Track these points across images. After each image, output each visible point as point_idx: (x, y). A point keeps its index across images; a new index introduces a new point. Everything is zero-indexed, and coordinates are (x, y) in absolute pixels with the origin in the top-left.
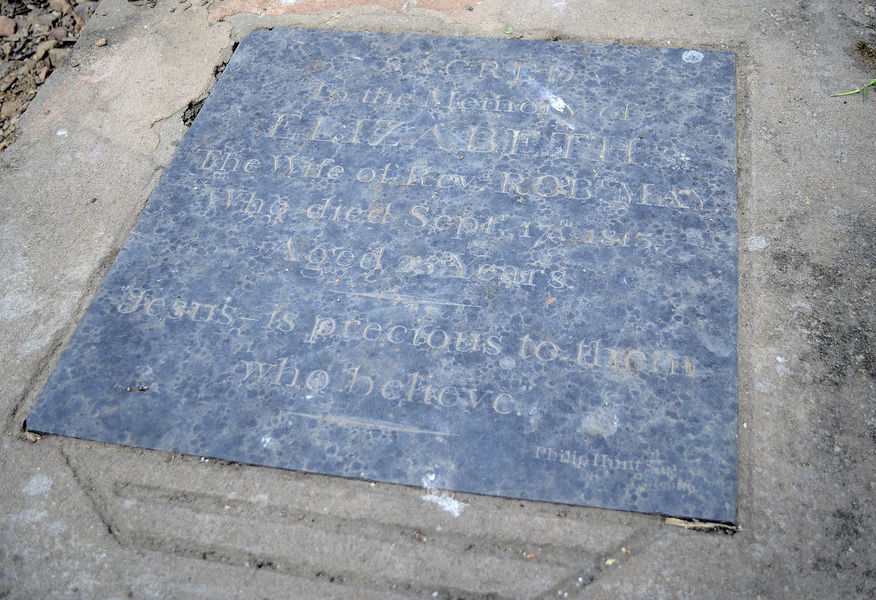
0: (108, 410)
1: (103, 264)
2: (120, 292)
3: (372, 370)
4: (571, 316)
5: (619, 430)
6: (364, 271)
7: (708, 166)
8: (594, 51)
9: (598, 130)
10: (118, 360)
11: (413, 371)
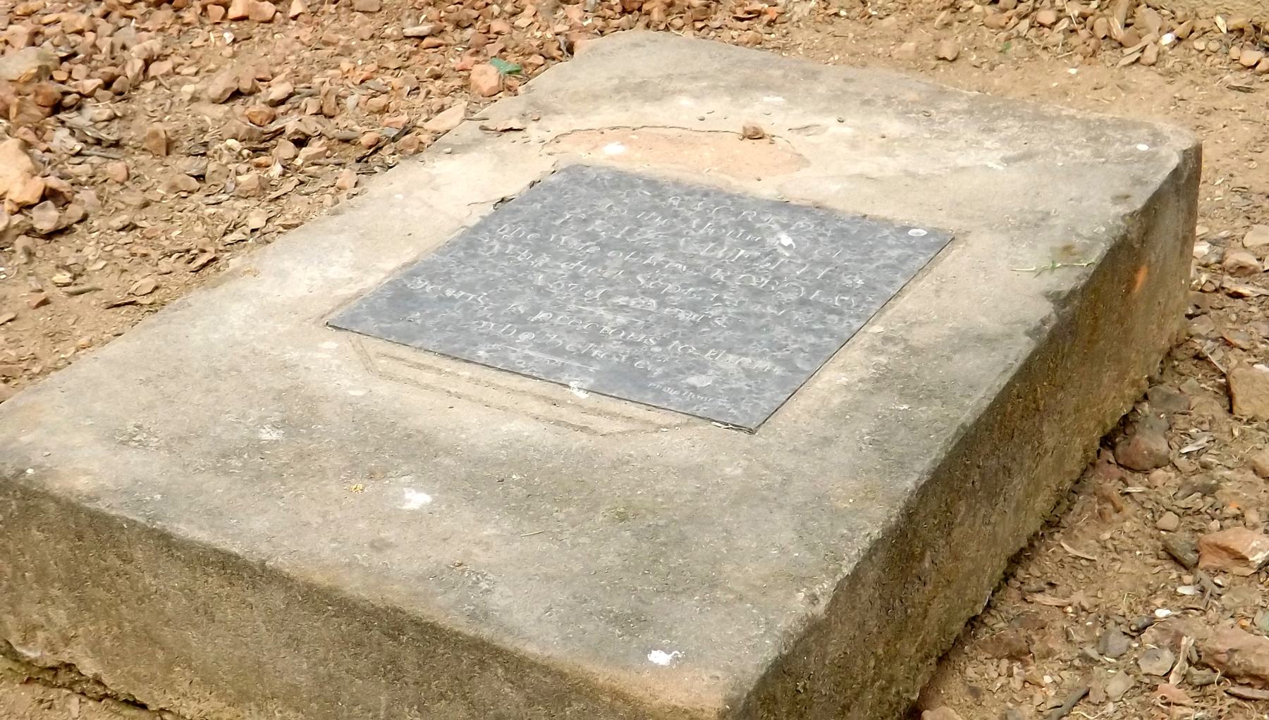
0: (383, 325)
1: (404, 266)
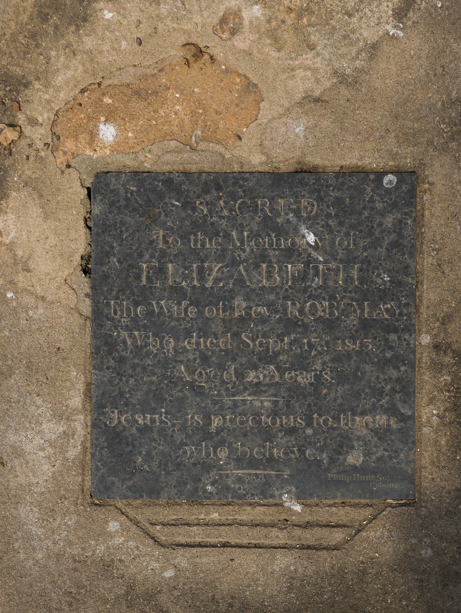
0: (130, 483)
2: (104, 413)
3: (247, 444)
4: (335, 400)
5: (363, 461)
6: (227, 383)
7: (400, 283)
8: (327, 182)
9: (336, 259)
10: (122, 455)
11: (267, 442)
